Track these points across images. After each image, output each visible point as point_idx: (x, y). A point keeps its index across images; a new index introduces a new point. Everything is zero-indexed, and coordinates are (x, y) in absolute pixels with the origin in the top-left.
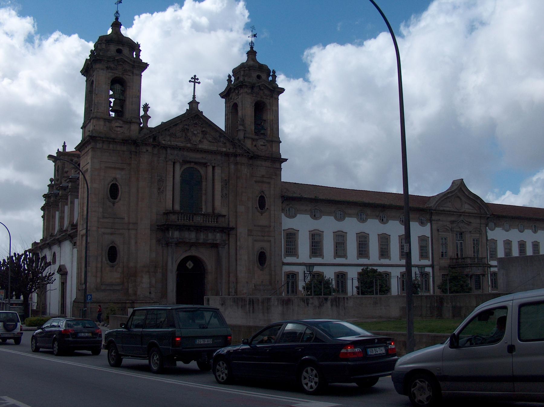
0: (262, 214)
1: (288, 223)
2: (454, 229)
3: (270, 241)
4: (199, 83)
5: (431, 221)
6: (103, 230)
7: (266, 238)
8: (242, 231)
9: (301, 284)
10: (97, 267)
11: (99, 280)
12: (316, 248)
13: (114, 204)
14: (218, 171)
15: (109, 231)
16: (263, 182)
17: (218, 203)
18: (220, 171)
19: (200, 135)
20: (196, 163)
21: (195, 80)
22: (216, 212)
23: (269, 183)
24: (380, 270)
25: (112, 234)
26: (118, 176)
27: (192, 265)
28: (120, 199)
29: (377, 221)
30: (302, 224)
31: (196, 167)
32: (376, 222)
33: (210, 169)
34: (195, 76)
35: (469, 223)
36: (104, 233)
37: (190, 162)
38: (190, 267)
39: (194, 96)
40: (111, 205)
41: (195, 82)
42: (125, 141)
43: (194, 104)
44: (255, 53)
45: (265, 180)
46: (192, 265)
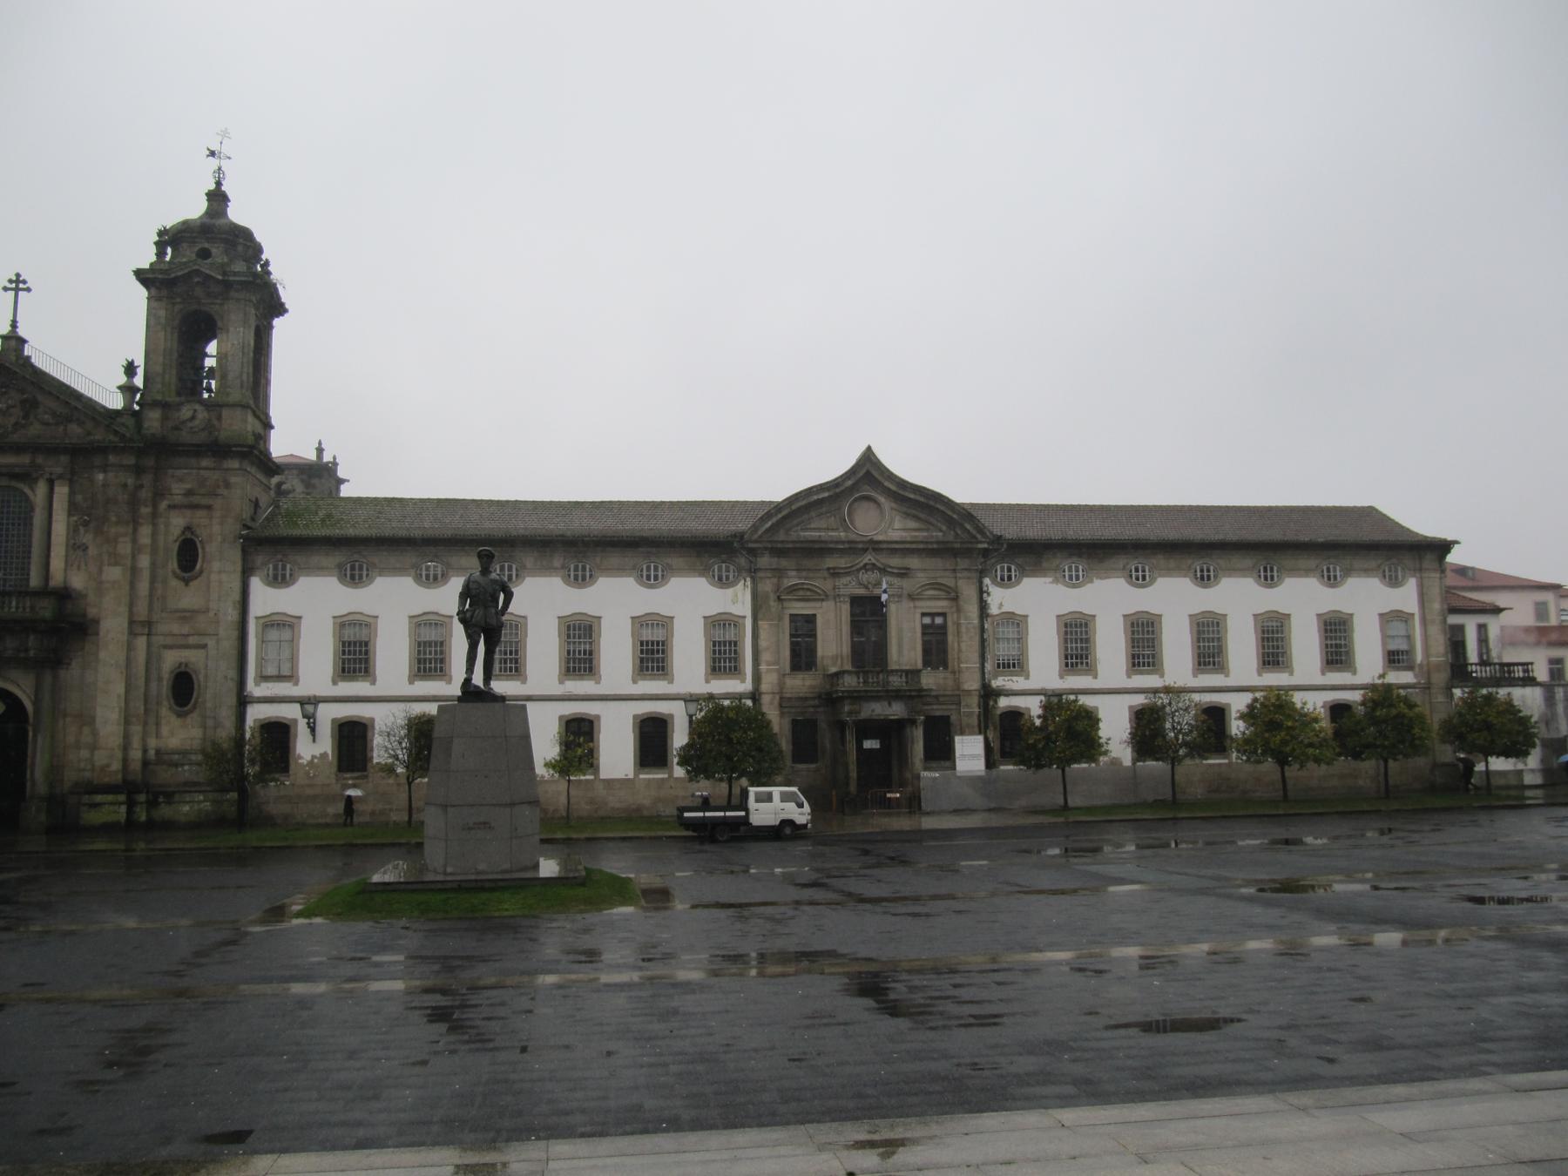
0: (187, 582)
1: (265, 599)
2: (842, 592)
4: (29, 290)
5: (753, 572)
7: (191, 640)
8: (113, 626)
9: (680, 738)
12: (355, 657)
14: (62, 491)
16: (194, 507)
17: (57, 564)
18: (66, 490)
21: (18, 285)
22: (52, 583)
23: (209, 507)
29: (1122, 581)
30: (314, 601)
34: (18, 275)
35: (904, 573)
39: (14, 324)
41: (17, 290)
45: (196, 500)
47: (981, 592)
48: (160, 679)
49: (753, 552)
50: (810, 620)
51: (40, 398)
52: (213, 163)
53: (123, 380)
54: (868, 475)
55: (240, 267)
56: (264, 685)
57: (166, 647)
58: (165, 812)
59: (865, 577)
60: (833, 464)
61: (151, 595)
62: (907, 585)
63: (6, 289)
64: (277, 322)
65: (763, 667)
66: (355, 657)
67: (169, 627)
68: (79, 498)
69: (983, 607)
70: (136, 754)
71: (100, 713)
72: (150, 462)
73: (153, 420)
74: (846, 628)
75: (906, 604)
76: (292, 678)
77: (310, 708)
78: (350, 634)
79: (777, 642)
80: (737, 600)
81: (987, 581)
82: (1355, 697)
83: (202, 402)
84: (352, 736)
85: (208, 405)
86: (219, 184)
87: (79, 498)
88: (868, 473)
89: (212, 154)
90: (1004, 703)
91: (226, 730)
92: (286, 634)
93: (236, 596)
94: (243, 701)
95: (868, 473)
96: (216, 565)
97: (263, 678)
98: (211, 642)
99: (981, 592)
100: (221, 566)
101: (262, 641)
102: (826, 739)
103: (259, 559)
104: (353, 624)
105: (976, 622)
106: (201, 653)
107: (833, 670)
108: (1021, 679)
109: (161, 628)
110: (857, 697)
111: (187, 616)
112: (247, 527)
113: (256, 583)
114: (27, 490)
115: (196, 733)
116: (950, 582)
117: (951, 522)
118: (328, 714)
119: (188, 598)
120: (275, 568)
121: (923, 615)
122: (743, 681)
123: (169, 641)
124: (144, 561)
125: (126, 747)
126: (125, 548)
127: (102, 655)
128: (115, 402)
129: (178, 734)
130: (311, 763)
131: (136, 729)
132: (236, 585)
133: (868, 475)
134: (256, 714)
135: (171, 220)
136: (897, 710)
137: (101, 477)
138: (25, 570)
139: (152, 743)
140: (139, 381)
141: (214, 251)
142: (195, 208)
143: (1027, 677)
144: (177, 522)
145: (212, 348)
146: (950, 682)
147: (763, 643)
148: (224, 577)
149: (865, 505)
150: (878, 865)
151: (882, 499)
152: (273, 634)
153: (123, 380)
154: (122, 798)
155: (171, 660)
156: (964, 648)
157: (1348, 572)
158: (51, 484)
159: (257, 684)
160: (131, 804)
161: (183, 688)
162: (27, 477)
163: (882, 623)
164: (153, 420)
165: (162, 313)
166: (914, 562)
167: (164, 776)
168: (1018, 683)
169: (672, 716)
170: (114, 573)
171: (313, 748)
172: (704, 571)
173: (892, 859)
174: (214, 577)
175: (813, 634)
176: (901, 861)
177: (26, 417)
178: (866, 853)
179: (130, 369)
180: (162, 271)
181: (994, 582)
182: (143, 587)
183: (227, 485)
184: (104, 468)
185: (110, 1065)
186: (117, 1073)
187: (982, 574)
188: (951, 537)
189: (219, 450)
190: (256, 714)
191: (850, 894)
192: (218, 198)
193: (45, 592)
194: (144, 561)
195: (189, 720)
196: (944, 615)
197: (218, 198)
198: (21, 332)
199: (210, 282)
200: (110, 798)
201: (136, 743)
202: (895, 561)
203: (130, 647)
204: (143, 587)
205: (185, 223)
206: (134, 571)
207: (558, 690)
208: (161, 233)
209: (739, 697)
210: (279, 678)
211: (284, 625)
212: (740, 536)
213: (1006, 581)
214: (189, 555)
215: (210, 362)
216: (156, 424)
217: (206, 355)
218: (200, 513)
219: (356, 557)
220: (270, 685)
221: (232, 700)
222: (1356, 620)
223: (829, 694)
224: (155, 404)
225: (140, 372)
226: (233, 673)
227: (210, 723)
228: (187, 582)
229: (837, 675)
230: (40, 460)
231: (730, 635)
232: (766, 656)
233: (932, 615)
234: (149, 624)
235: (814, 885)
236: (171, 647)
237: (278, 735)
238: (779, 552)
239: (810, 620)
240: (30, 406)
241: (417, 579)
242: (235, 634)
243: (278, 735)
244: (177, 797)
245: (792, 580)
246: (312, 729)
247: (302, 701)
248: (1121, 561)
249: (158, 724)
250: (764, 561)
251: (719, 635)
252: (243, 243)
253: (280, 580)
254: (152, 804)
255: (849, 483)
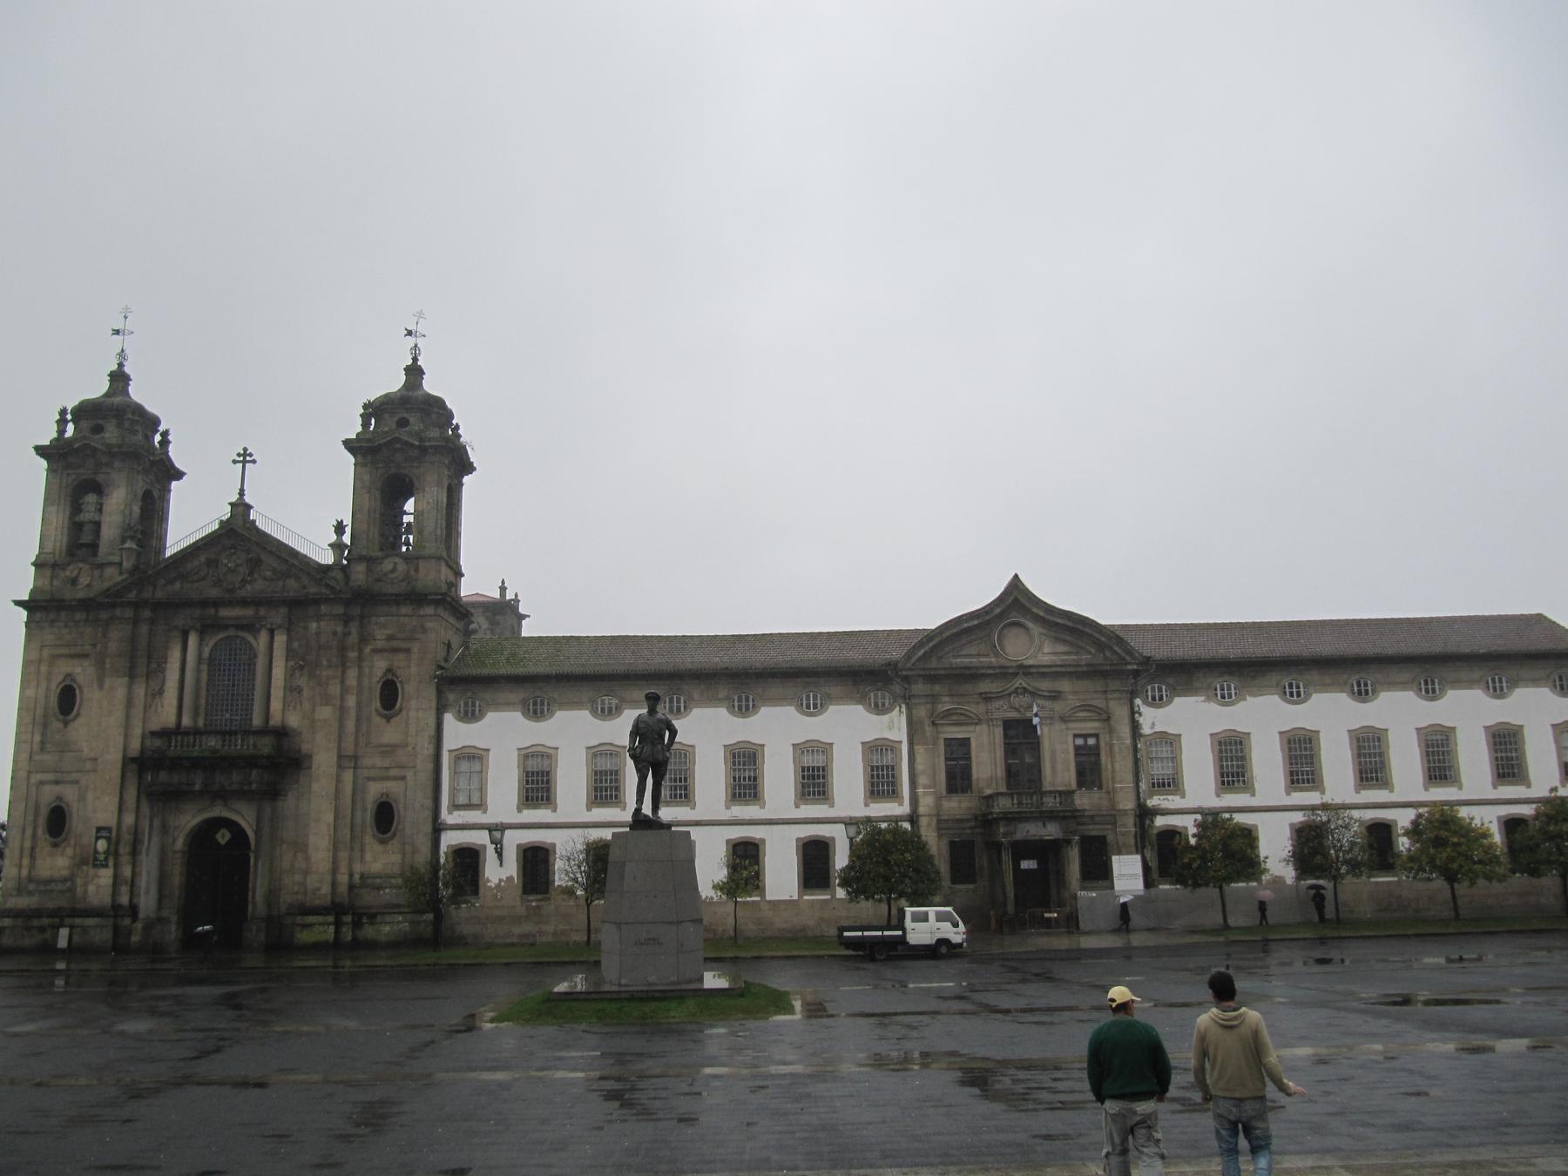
0: (388, 719)
1: (457, 733)
3: (403, 778)
4: (254, 462)
5: (907, 699)
6: (39, 777)
7: (393, 772)
8: (323, 760)
10: (22, 850)
11: (25, 872)
12: (537, 786)
13: (66, 724)
14: (280, 639)
15: (51, 777)
16: (395, 650)
17: (276, 705)
18: (284, 638)
19: (243, 570)
20: (239, 627)
21: (245, 458)
22: (271, 723)
23: (408, 651)
24: (1239, 818)
25: (57, 782)
26: (78, 670)
27: (219, 837)
28: (78, 715)
30: (501, 734)
31: (240, 634)
32: (516, 717)
33: (263, 637)
34: (245, 449)
35: (1055, 696)
36: (42, 783)
37: (226, 627)
38: (223, 841)
40: (61, 725)
41: (244, 462)
42: (88, 605)
43: (241, 508)
44: (421, 372)
45: (395, 644)
46: (228, 836)
47: (1133, 712)
48: (364, 810)
49: (906, 679)
50: (965, 743)
51: (263, 556)
52: (411, 341)
53: (334, 538)
54: (1017, 602)
55: (434, 433)
56: (456, 813)
57: (369, 779)
58: (368, 932)
59: (1016, 701)
60: (982, 593)
61: (357, 731)
62: (1059, 707)
63: (235, 462)
64: (466, 479)
65: (920, 790)
66: (537, 786)
67: (373, 760)
68: (296, 644)
69: (1135, 727)
70: (343, 878)
71: (312, 839)
72: (356, 611)
73: (359, 573)
74: (1000, 753)
75: (1058, 726)
76: (481, 806)
77: (497, 834)
78: (533, 765)
79: (933, 764)
80: (893, 726)
81: (1138, 701)
82: (1527, 810)
83: (401, 555)
84: (536, 861)
85: (407, 558)
86: (415, 359)
87: (296, 644)
88: (1016, 600)
89: (410, 333)
90: (1160, 821)
91: (422, 857)
92: (477, 767)
93: (431, 731)
94: (438, 829)
95: (1016, 600)
96: (413, 703)
97: (455, 807)
98: (409, 774)
99: (1133, 713)
100: (417, 703)
101: (455, 773)
102: (982, 861)
103: (451, 697)
104: (534, 755)
105: (1128, 741)
106: (402, 783)
107: (988, 792)
108: (1177, 798)
109: (366, 762)
110: (1011, 818)
111: (390, 750)
112: (441, 668)
113: (449, 718)
114: (251, 639)
115: (396, 858)
116: (1100, 703)
117: (1101, 647)
118: (513, 840)
119: (389, 734)
120: (466, 704)
121: (1076, 736)
122: (901, 804)
123: (373, 773)
124: (351, 701)
125: (334, 871)
126: (334, 689)
127: (315, 787)
128: (327, 558)
129: (380, 859)
130: (498, 885)
131: (343, 855)
132: (432, 721)
133: (1017, 602)
134: (449, 840)
135: (374, 395)
136: (1051, 831)
137: (314, 625)
138: (248, 709)
139: (357, 868)
140: (347, 539)
141: (412, 420)
142: (394, 382)
143: (1183, 797)
144: (380, 665)
145: (410, 505)
146: (1105, 803)
147: (919, 767)
148: (420, 714)
149: (1015, 630)
150: (1024, 981)
151: (1030, 625)
152: (464, 766)
153: (334, 538)
154: (331, 919)
155: (374, 790)
156: (1117, 768)
157: (1514, 683)
158: (272, 632)
159: (450, 813)
160: (338, 924)
161: (385, 816)
162: (251, 627)
163: (1035, 744)
164: (359, 573)
165: (367, 477)
166: (1065, 685)
167: (368, 898)
168: (1173, 802)
169: (833, 839)
170: (325, 713)
171: (499, 872)
172: (862, 699)
173: (1037, 975)
174: (412, 714)
175: (967, 757)
176: (1048, 978)
177: (251, 574)
178: (1015, 970)
179: (340, 528)
180: (369, 440)
181: (1145, 702)
182: (350, 725)
183: (424, 630)
184: (319, 618)
185: (358, 1125)
186: (363, 1130)
187: (1133, 694)
188: (1099, 659)
189: (417, 598)
190: (449, 840)
191: (987, 1006)
192: (414, 372)
193: (265, 731)
194: (351, 701)
195: (389, 847)
196: (1096, 736)
197: (414, 372)
198: (247, 499)
199: (409, 447)
200: (320, 919)
201: (343, 868)
202: (1045, 685)
203: (339, 781)
204: (350, 725)
205: (386, 396)
206: (342, 710)
207: (725, 815)
208: (365, 407)
209: (897, 819)
210: (469, 806)
211: (473, 757)
212: (893, 665)
213: (1157, 702)
214: (390, 694)
215: (407, 519)
216: (361, 577)
217: (405, 513)
218: (401, 656)
219: (538, 693)
220: (462, 813)
221: (428, 828)
222: (1526, 731)
223: (985, 815)
224: (361, 559)
225: (348, 530)
226: (429, 803)
227: (408, 848)
228: (388, 719)
229: (990, 797)
230: (262, 612)
231: (888, 759)
232: (922, 780)
233: (1085, 736)
234: (356, 758)
235: (960, 998)
236: (374, 779)
237: (469, 859)
238: (932, 678)
239: (965, 743)
240: (255, 564)
241: (594, 712)
242: (431, 766)
243: (469, 859)
244: (379, 919)
245: (946, 705)
246: (500, 854)
247: (491, 829)
248: (1274, 677)
249: (362, 851)
250: (919, 688)
251: (876, 760)
252: (437, 411)
253: (470, 715)
254: (357, 924)
255: (998, 610)
